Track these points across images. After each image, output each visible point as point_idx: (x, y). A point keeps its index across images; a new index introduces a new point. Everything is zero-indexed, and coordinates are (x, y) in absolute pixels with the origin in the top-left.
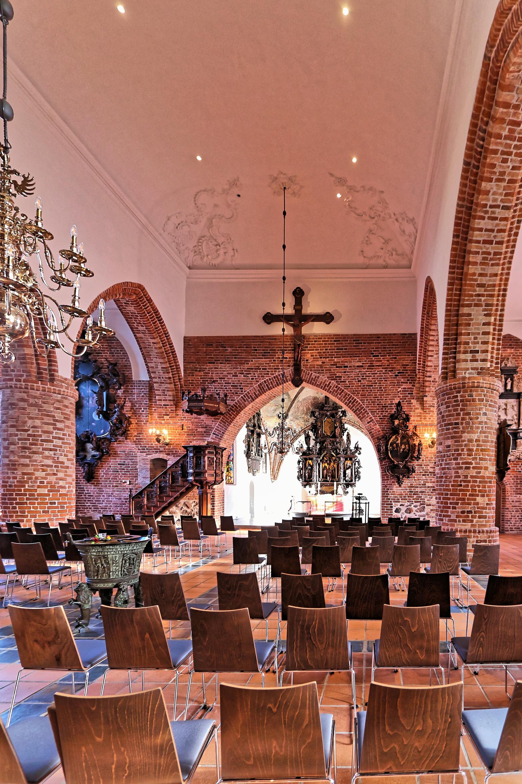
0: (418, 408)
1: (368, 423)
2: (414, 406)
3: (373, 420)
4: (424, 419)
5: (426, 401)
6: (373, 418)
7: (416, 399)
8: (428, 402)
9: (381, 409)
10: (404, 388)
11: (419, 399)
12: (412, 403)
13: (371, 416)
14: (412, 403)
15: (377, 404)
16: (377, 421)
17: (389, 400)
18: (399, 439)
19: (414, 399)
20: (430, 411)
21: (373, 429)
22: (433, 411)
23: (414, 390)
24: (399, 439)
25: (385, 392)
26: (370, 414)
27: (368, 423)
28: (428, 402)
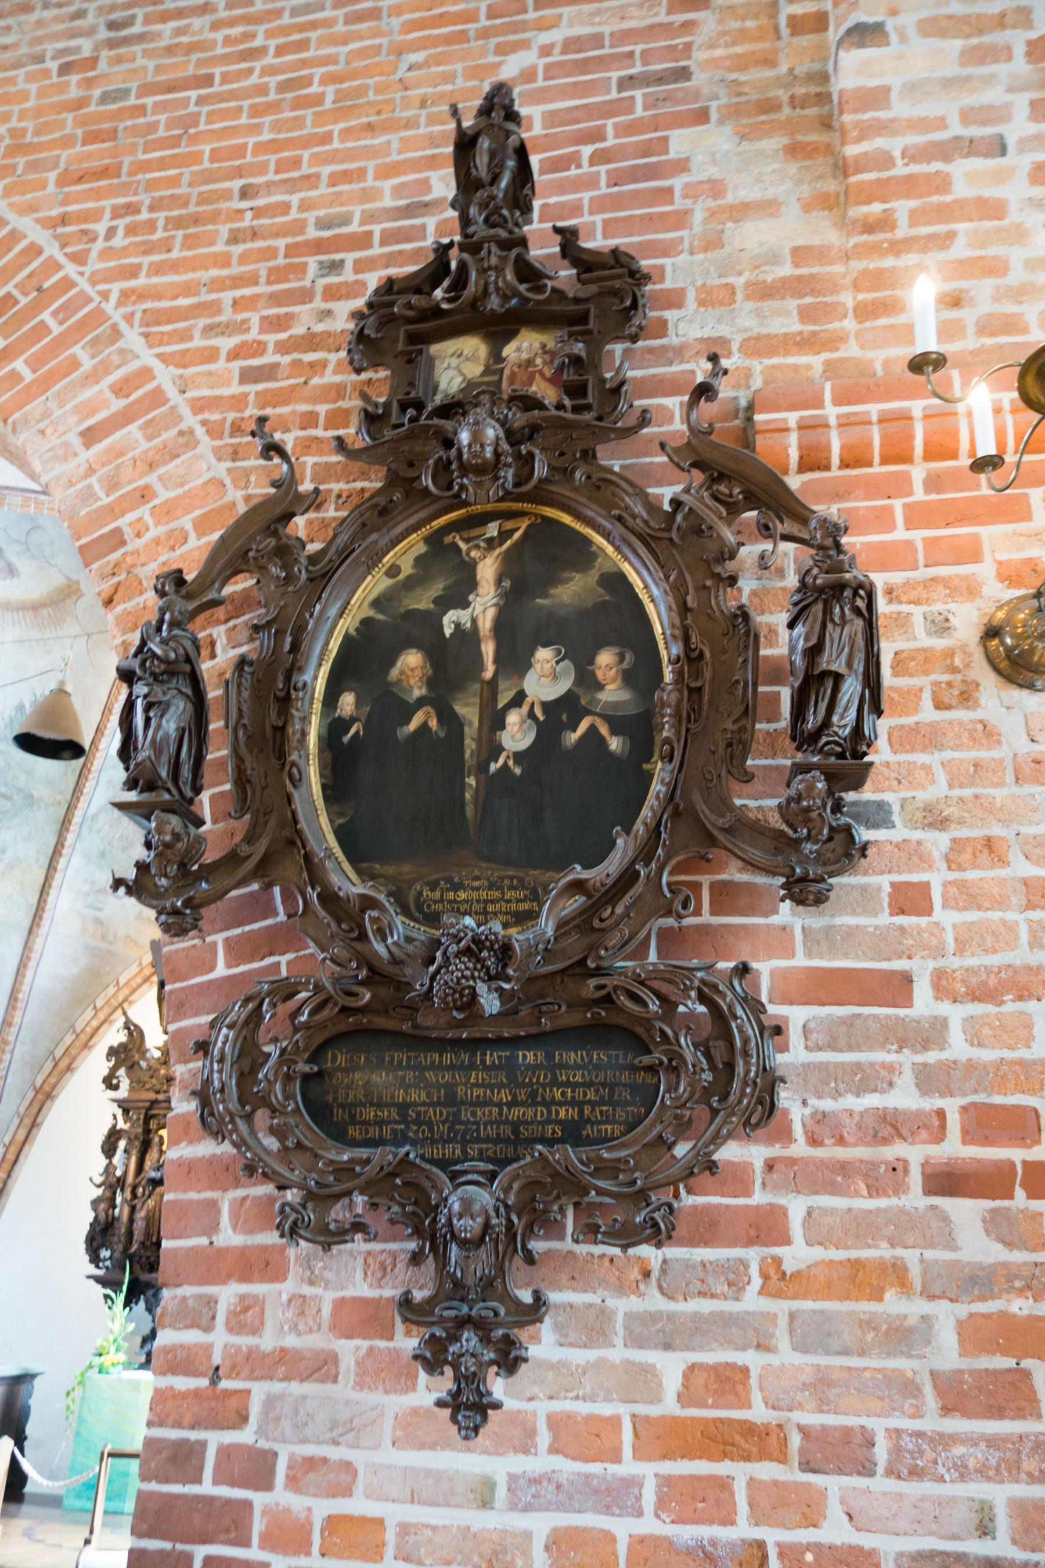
0: (769, 207)
1: (90, 437)
2: (715, 188)
3: (158, 397)
4: (863, 312)
5: (878, 97)
6: (165, 377)
7: (732, 113)
8: (900, 109)
9: (277, 275)
10: (571, 45)
11: (769, 106)
12: (682, 166)
13: (147, 357)
14: (682, 166)
15: (234, 238)
16: (199, 406)
17: (386, 172)
18: (487, 570)
19: (701, 117)
20: (946, 213)
21: (144, 495)
22: (993, 209)
23: (698, 39)
24: (487, 570)
25: (340, 113)
26: (133, 338)
27: (90, 437)
28: (900, 109)
